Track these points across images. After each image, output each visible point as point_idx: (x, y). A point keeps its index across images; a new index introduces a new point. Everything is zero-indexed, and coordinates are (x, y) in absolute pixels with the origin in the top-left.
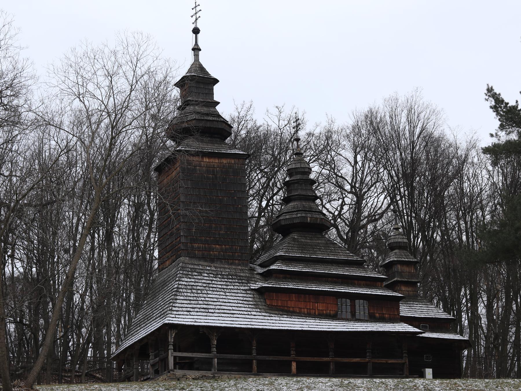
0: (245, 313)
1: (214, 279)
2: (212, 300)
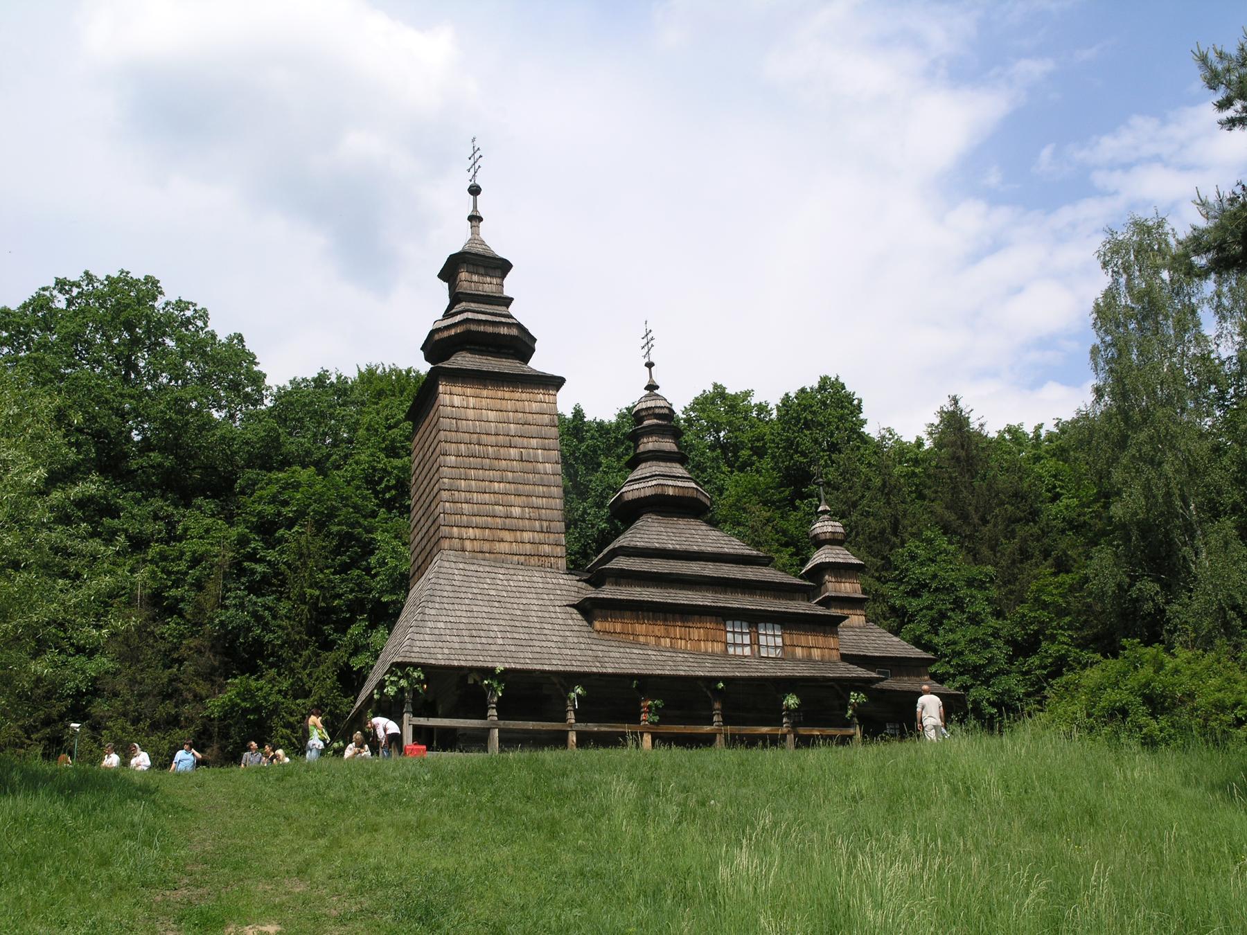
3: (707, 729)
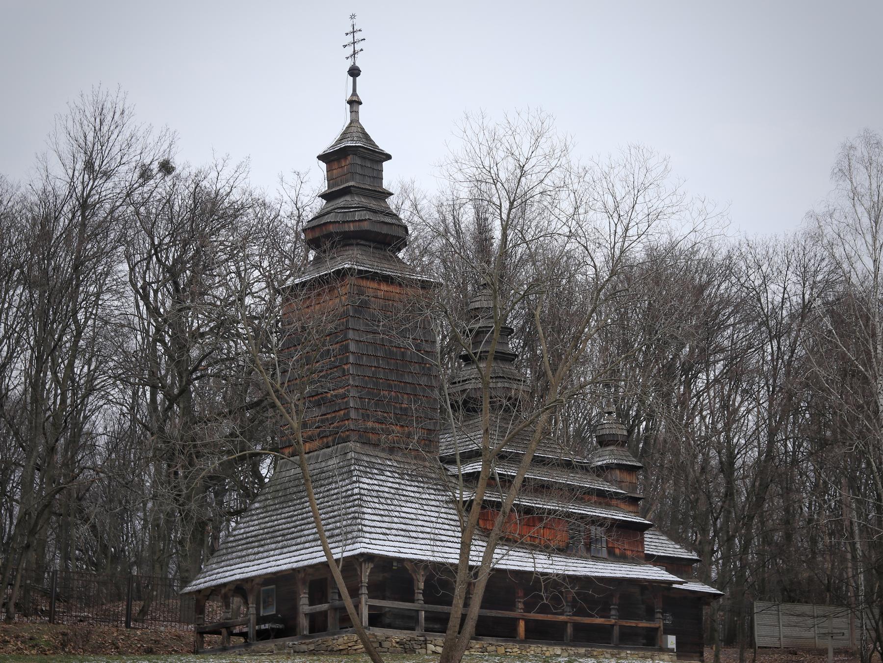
3: (562, 618)
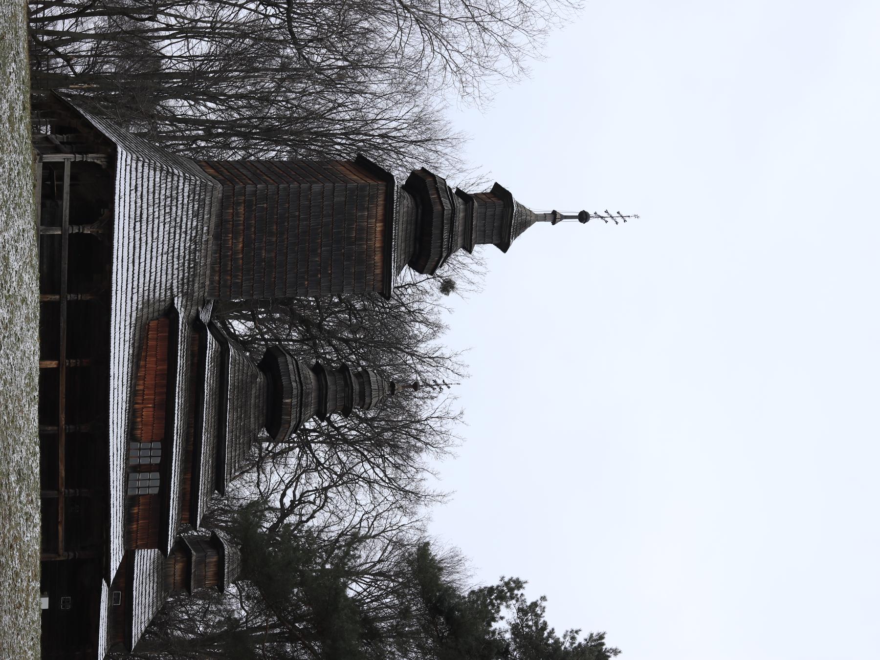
0: (135, 283)
1: (188, 237)
2: (156, 229)
3: (62, 417)
